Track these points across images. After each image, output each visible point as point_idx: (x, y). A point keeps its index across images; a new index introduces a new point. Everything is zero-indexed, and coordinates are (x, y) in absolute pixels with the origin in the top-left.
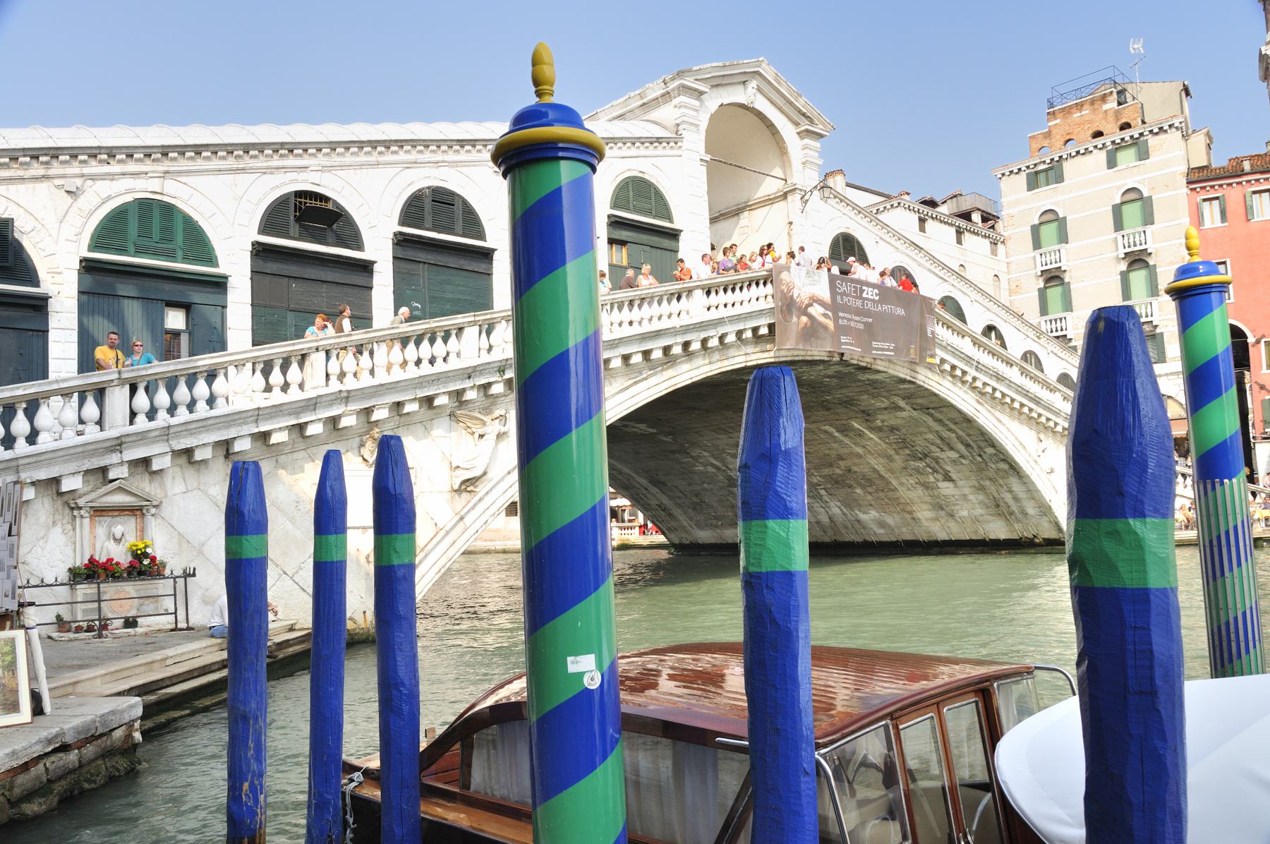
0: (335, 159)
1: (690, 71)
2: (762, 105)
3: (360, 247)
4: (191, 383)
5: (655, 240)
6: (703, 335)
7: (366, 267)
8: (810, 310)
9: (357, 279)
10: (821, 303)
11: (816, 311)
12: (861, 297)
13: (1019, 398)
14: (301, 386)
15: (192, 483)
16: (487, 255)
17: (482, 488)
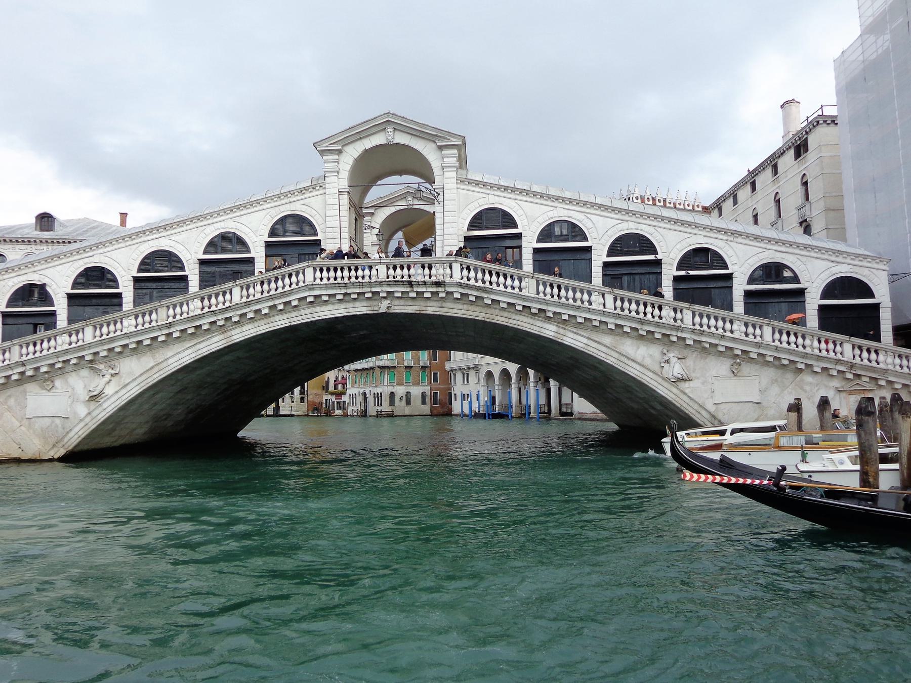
2: (401, 139)
3: (117, 287)
9: (116, 301)
13: (612, 320)
17: (102, 401)
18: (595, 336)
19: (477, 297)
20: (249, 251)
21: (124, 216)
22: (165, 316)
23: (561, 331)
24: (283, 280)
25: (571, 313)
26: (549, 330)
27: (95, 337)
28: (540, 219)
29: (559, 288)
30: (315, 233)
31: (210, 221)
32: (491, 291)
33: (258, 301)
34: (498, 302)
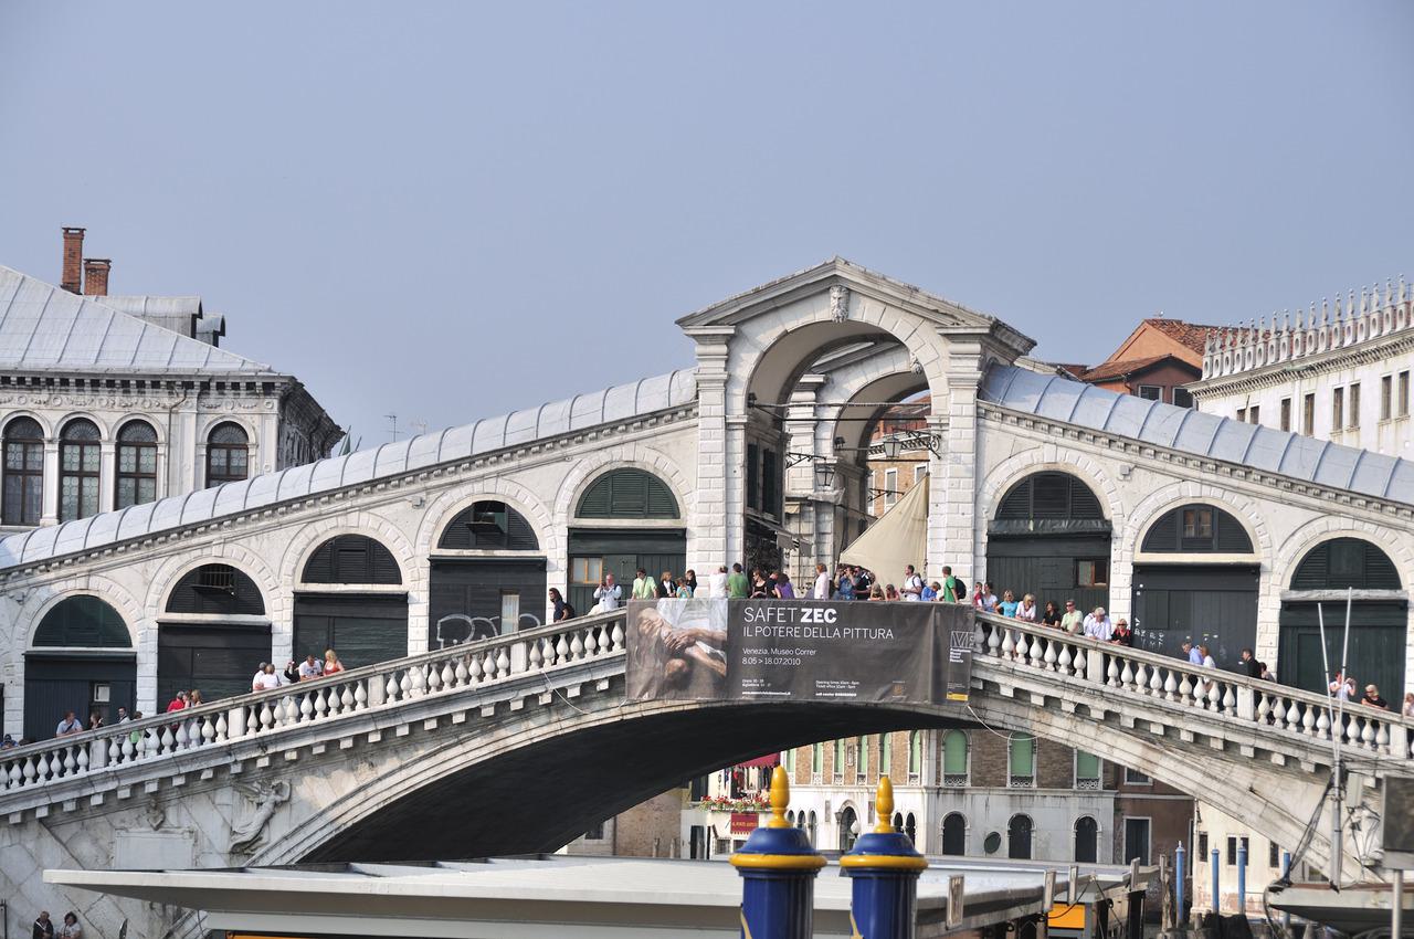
0: (238, 529)
1: (692, 317)
2: (867, 313)
3: (262, 612)
4: (36, 761)
5: (645, 545)
6: (523, 694)
7: (266, 631)
8: (689, 650)
10: (712, 641)
11: (701, 651)
12: (797, 622)
13: (1251, 741)
14: (87, 768)
15: (16, 839)
16: (402, 600)
18: (1217, 767)
19: (986, 682)
20: (533, 544)
21: (74, 237)
22: (380, 697)
23: (1153, 756)
24: (609, 632)
25: (1169, 721)
26: (1126, 752)
27: (246, 729)
28: (1151, 503)
29: (1149, 673)
30: (674, 512)
31: (456, 478)
32: (1012, 673)
33: (561, 674)
34: (1028, 693)
